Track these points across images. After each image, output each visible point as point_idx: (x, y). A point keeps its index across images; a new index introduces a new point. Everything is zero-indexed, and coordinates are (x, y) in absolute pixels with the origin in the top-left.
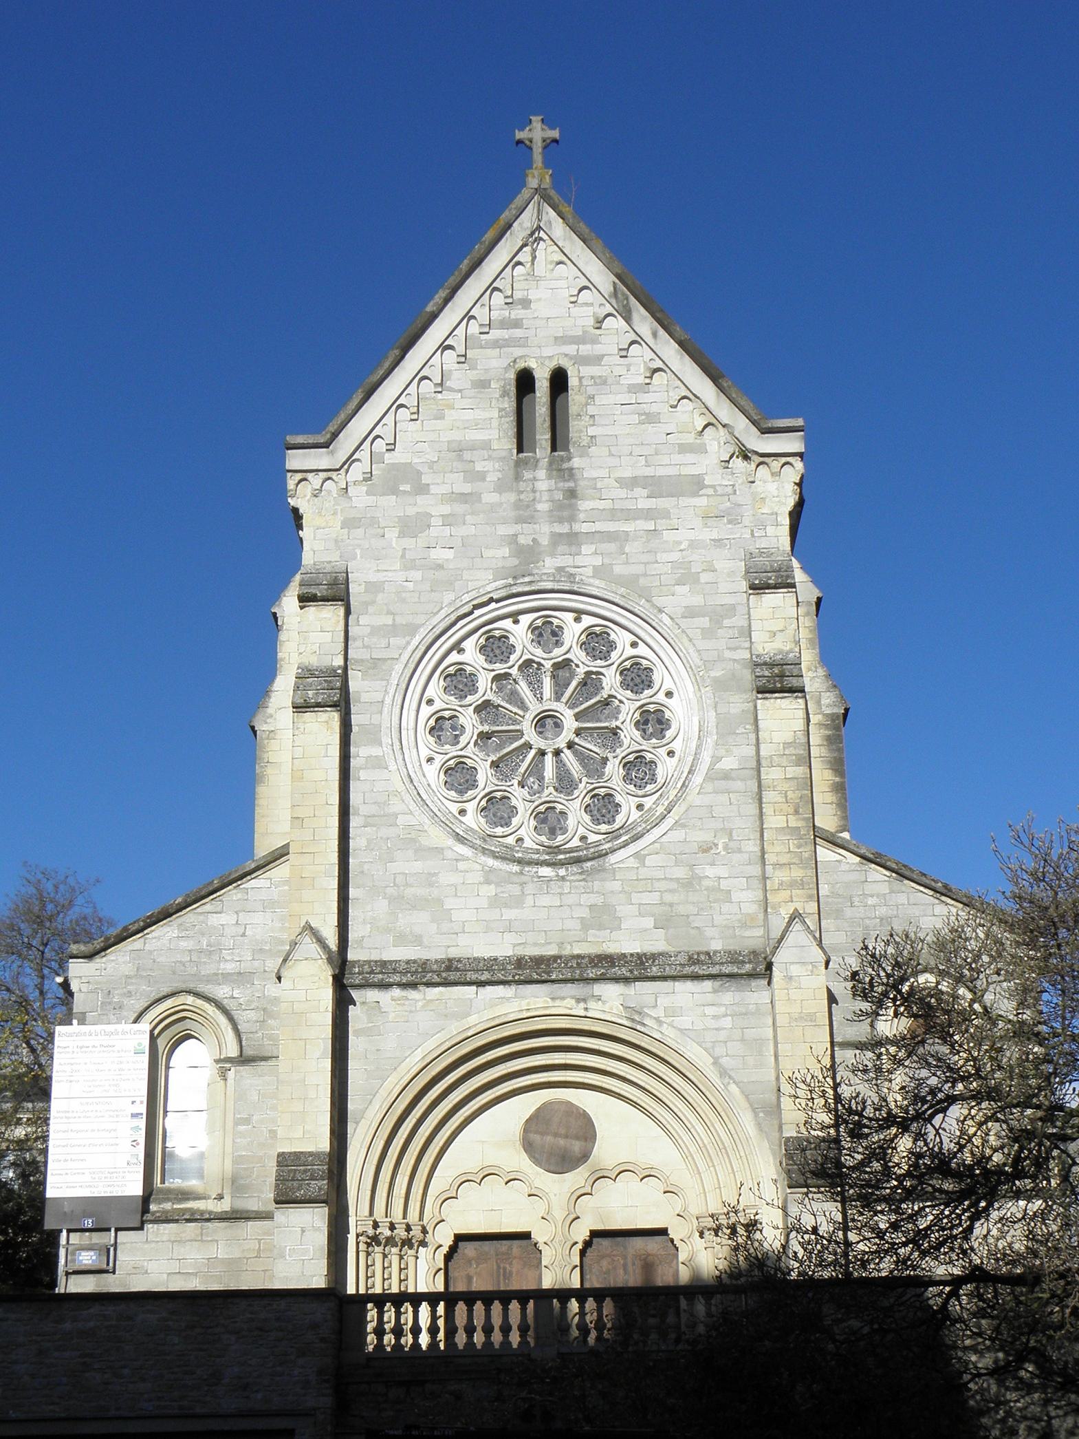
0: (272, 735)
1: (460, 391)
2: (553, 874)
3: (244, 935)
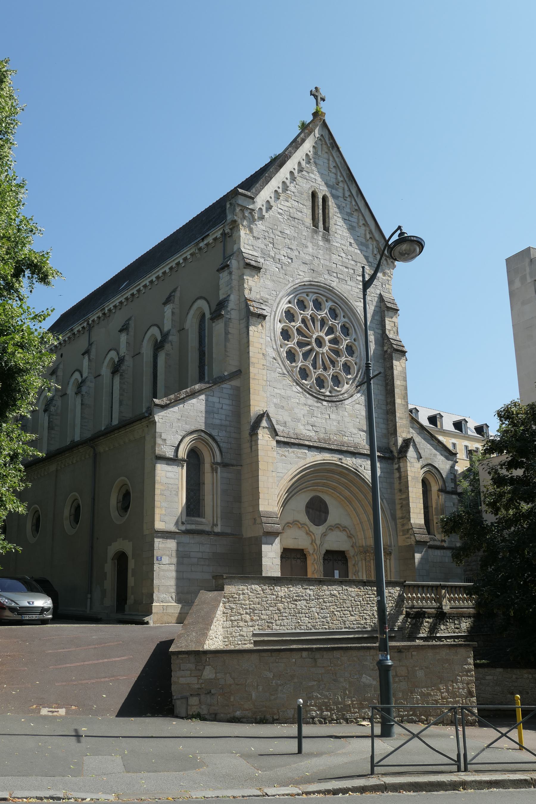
0: (230, 321)
1: (293, 193)
2: (327, 405)
3: (222, 408)
